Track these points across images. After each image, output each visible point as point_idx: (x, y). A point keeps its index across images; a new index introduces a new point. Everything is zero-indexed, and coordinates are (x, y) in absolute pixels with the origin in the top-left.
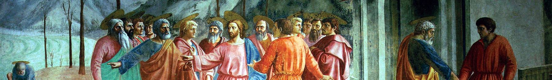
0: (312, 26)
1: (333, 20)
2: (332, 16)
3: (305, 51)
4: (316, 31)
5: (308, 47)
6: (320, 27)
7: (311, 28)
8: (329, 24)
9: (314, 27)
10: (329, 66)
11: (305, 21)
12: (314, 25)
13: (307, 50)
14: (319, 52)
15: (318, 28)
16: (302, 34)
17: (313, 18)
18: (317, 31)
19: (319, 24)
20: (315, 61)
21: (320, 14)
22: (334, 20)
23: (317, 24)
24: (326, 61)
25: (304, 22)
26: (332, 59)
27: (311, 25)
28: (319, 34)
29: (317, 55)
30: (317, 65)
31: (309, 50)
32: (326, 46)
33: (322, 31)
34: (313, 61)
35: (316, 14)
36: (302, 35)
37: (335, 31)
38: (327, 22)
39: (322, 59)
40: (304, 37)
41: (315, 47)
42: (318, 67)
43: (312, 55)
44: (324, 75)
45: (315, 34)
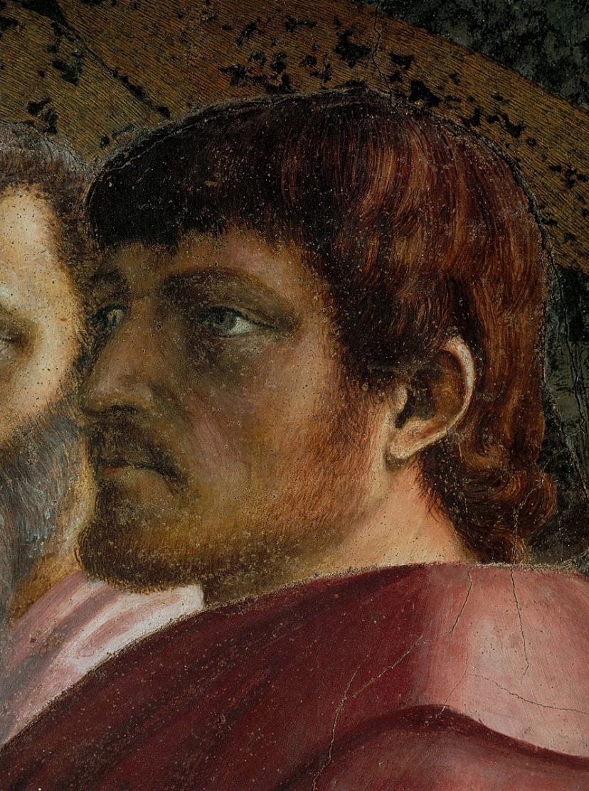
2: (350, 52)
22: (422, 161)
33: (85, 487)
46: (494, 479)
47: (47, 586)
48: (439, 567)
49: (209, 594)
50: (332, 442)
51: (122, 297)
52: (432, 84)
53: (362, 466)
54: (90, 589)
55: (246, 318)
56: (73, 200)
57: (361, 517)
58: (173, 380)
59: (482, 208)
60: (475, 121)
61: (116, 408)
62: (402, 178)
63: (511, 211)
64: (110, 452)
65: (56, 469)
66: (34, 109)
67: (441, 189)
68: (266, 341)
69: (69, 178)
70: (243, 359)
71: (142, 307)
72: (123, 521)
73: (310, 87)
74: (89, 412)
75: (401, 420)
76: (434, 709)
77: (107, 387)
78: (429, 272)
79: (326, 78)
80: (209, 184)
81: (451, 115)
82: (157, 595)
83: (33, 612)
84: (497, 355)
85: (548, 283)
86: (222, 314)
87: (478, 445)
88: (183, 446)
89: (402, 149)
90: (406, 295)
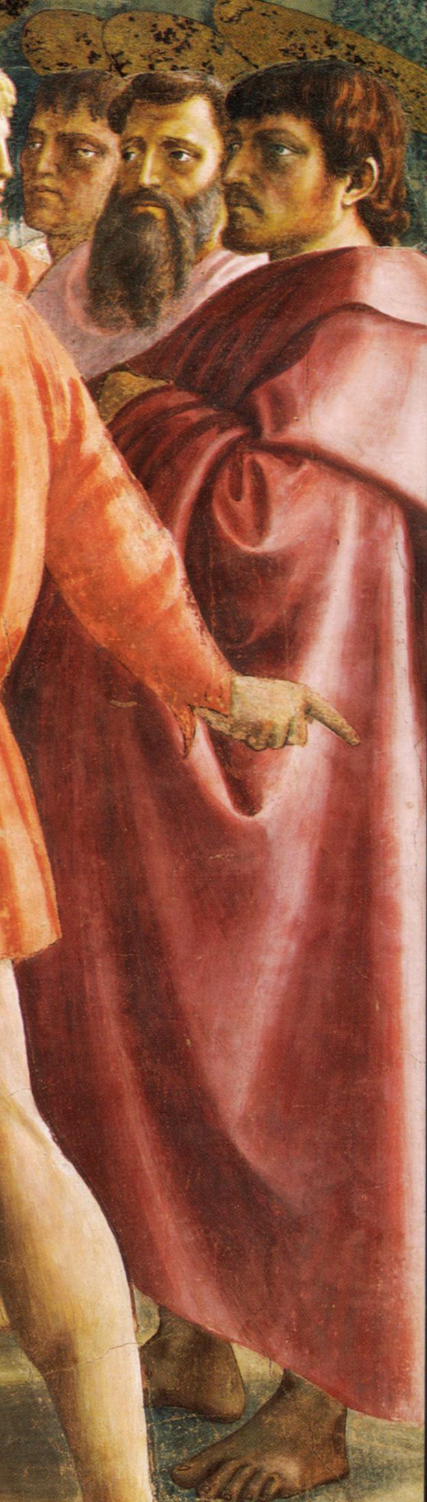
0: (125, 156)
1: (344, 91)
2: (330, 43)
3: (48, 416)
4: (158, 213)
5: (77, 376)
6: (206, 171)
7: (106, 170)
8: (296, 128)
9: (139, 167)
10: (297, 577)
11: (50, 103)
12: (142, 146)
13: (62, 413)
14: (200, 428)
15: (185, 172)
16: (13, 236)
17: (136, 69)
18: (178, 209)
19: (191, 137)
20: (152, 528)
21: (208, 22)
22: (358, 87)
23: (170, 129)
24: (262, 527)
25: (32, 113)
26: (335, 505)
27: (111, 140)
28: (200, 243)
29: (167, 461)
30: (168, 567)
31: (89, 407)
32: (276, 365)
34: (128, 524)
35: (165, 23)
36: (15, 253)
37: (364, 211)
38: (273, 107)
39: (227, 508)
40: (34, 274)
41: (152, 375)
42: (177, 587)
43: (113, 465)
44: (241, 682)
45: (154, 239)
46: (385, 213)
47: (207, 253)
48: (362, 248)
49: (271, 257)
50: (322, 198)
51: (239, 139)
52: (363, 57)
53: (331, 208)
54: (226, 253)
55: (288, 149)
56: (219, 101)
57: (332, 228)
58: (258, 172)
59: (383, 107)
60: (380, 71)
61: (235, 183)
62: (350, 95)
63: (396, 107)
64: (233, 200)
65: (212, 206)
66: (204, 65)
67: (367, 100)
68: (295, 157)
69: (219, 92)
70: (287, 165)
71: (246, 143)
72: (238, 227)
73: (315, 58)
74: (224, 184)
75: (348, 189)
76: (359, 304)
77: (232, 174)
78: (361, 131)
79: (321, 54)
80: (274, 95)
81: (370, 69)
82: (251, 257)
83: (203, 261)
84: (387, 164)
85: (408, 137)
86: (279, 147)
87: (380, 200)
88: (260, 198)
89: (352, 83)
90: (352, 139)
